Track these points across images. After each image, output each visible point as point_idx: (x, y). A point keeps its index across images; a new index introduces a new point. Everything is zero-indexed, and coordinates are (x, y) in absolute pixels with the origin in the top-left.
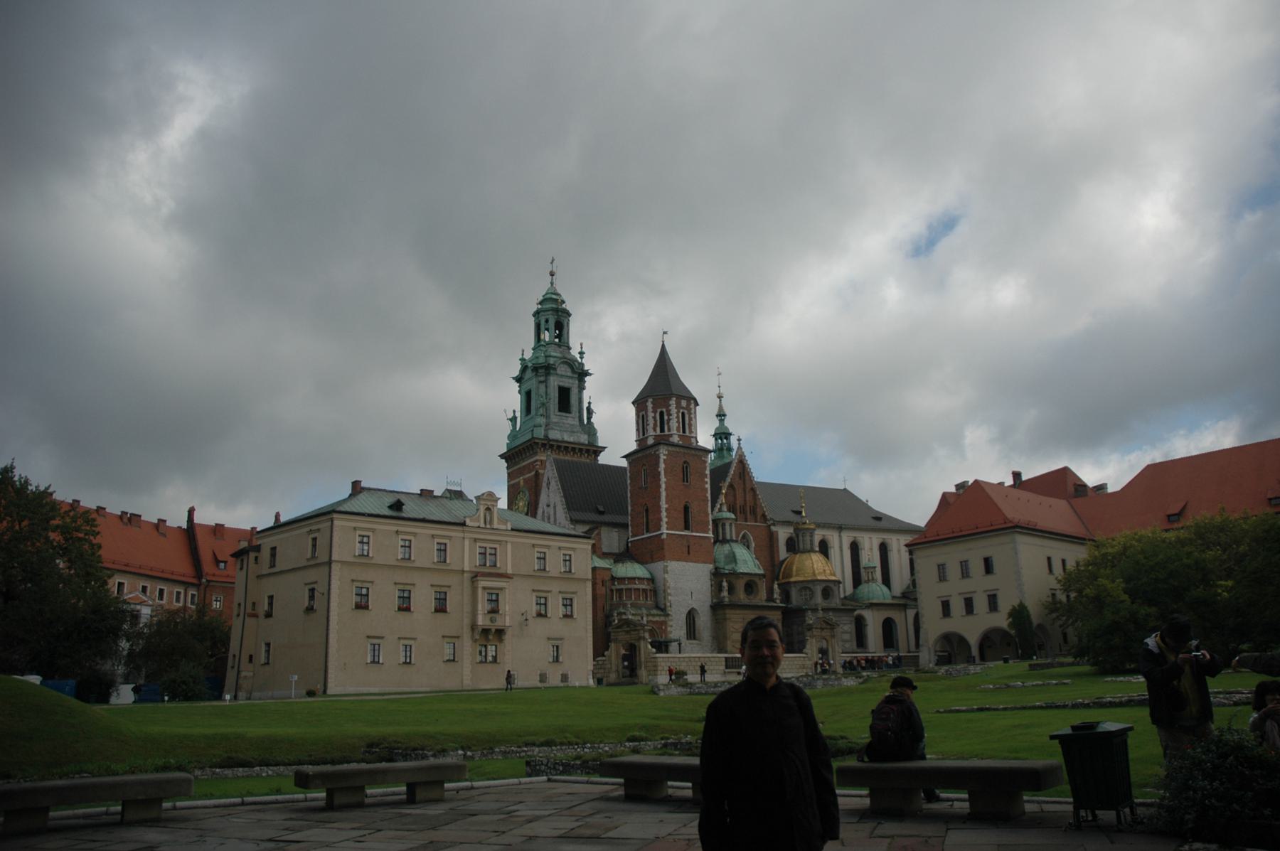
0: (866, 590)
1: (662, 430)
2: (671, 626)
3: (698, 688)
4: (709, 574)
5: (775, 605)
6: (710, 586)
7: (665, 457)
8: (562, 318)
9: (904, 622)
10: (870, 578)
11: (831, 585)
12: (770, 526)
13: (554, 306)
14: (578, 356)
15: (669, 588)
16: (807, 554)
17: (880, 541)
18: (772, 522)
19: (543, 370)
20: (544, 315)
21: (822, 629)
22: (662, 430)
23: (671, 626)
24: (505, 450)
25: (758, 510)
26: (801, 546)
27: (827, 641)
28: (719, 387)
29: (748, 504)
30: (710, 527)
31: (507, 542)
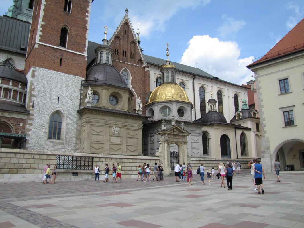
2: (31, 124)
4: (80, 85)
6: (79, 95)
9: (234, 137)
11: (186, 106)
12: (144, 67)
15: (33, 90)
16: (168, 84)
18: (146, 65)
21: (175, 135)
23: (31, 124)
26: (165, 80)
27: (179, 146)
28: (138, 29)
29: (129, 51)
30: (86, 49)
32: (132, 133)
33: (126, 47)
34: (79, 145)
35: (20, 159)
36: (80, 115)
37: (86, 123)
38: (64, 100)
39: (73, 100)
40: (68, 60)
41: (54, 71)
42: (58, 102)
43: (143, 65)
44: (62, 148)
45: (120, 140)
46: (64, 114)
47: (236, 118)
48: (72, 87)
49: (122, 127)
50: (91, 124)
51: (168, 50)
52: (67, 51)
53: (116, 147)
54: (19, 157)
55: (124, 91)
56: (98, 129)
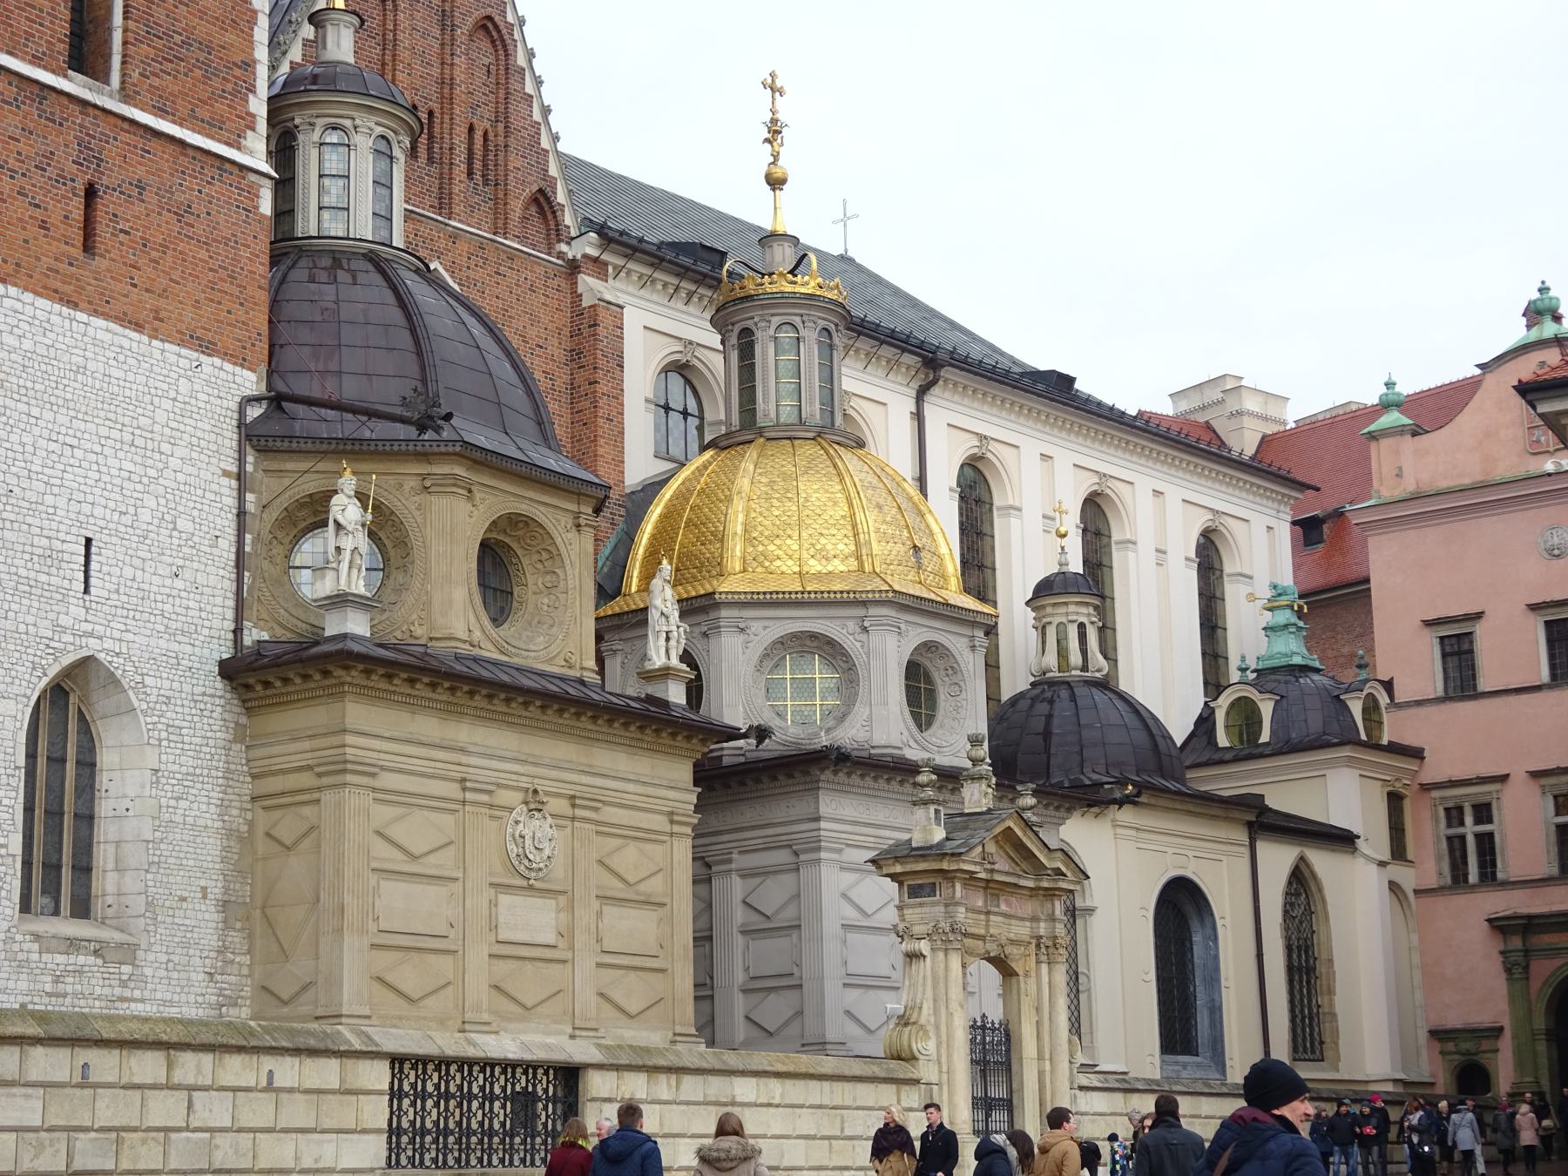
16: (809, 450)
17: (1087, 485)
18: (588, 246)
25: (515, 161)
30: (258, 106)
32: (629, 859)
33: (436, 71)
34: (241, 965)
35: (195, 1094)
36: (244, 701)
37: (320, 775)
38: (128, 572)
39: (187, 574)
40: (139, 208)
41: (48, 298)
42: (86, 591)
43: (563, 247)
44: (127, 993)
45: (553, 923)
46: (131, 693)
47: (1222, 740)
48: (179, 452)
49: (569, 812)
50: (374, 789)
51: (775, 131)
52: (132, 122)
53: (529, 983)
54: (190, 1080)
55: (573, 507)
56: (418, 831)
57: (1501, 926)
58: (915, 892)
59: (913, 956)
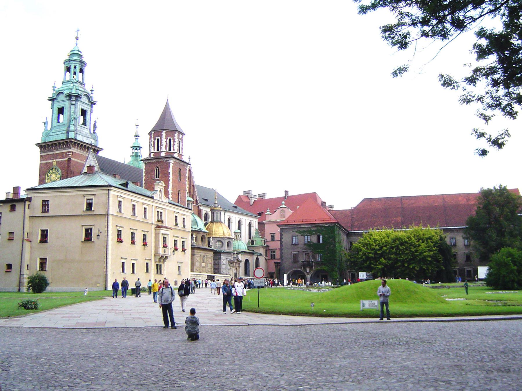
0: (237, 244)
1: (170, 149)
3: (323, 290)
5: (211, 248)
7: (172, 165)
8: (83, 67)
9: (252, 260)
10: (238, 238)
11: (231, 241)
12: (199, 206)
13: (80, 59)
14: (90, 92)
16: (219, 223)
19: (75, 98)
20: (74, 63)
21: (236, 263)
22: (170, 149)
24: (40, 141)
26: (215, 219)
31: (166, 209)
53: (204, 269)
57: (275, 263)
58: (231, 263)
59: (231, 268)
